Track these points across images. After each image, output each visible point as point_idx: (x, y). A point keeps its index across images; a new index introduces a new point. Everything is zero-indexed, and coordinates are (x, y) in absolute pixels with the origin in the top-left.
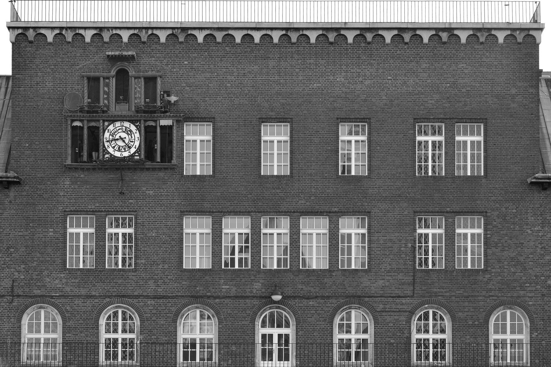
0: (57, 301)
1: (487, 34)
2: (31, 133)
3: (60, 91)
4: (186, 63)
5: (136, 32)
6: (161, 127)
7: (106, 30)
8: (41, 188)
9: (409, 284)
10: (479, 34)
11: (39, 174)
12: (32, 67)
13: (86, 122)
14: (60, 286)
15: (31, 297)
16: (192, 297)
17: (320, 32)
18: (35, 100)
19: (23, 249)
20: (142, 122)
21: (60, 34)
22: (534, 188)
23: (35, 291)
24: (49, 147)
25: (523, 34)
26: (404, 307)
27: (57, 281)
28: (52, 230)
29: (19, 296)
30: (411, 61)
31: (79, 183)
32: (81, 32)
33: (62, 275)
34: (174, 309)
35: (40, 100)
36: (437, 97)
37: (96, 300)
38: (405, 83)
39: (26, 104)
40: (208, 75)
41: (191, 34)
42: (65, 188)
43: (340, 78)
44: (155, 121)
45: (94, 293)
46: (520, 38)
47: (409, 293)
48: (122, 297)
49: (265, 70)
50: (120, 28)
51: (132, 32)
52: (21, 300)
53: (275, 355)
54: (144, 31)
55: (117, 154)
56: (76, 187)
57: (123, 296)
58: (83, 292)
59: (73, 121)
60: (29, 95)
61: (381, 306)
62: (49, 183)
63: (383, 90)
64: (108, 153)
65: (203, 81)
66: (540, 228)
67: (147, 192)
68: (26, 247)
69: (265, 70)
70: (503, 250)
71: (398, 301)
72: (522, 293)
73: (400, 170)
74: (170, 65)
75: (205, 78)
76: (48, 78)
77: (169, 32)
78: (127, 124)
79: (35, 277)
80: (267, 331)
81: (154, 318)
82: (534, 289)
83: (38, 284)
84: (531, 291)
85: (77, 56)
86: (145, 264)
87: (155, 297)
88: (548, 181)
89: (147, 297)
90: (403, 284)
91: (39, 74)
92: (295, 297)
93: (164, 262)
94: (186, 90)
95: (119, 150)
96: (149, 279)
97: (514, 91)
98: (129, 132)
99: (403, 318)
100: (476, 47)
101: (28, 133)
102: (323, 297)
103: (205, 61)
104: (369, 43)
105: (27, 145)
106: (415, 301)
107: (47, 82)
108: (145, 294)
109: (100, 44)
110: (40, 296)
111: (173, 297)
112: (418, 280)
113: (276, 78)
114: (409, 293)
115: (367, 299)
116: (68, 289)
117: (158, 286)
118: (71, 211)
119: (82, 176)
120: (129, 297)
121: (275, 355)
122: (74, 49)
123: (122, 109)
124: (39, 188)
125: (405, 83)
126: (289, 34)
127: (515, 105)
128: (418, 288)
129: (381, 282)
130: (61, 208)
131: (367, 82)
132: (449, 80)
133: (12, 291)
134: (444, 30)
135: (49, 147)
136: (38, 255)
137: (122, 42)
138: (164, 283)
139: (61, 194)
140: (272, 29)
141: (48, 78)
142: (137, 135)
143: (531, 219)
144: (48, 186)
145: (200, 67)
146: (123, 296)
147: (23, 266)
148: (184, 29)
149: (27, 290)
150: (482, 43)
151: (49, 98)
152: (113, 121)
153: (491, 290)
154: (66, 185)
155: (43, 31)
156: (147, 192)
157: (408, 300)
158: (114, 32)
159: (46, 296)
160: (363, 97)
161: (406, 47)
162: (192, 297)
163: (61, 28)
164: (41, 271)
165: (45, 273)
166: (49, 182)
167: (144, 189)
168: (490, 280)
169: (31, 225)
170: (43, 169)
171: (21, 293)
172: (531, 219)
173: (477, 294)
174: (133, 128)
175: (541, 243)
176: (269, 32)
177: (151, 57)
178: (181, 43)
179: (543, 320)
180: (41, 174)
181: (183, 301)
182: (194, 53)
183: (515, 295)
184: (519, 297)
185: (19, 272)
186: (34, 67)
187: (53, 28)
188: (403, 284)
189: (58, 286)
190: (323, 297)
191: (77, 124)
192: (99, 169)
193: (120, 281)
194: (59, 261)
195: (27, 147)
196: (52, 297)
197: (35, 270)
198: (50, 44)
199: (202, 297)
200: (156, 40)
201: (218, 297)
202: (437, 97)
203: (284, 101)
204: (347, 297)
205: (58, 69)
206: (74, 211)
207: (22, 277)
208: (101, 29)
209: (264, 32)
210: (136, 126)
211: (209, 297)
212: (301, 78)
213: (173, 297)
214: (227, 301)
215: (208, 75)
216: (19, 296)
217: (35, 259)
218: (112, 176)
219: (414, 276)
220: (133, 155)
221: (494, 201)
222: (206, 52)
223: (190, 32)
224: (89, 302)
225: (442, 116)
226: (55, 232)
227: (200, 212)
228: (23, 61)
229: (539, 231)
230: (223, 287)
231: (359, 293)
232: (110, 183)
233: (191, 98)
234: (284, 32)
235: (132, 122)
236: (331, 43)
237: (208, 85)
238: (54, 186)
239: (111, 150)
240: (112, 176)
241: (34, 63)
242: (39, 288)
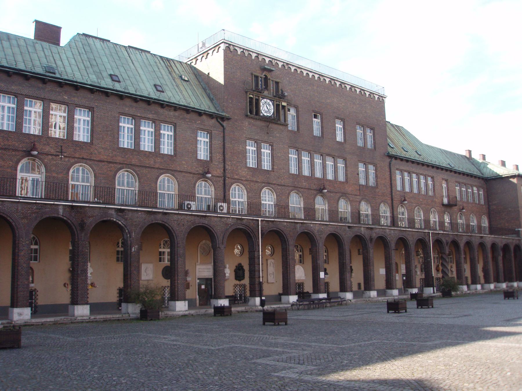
5: (271, 60)
7: (260, 55)
13: (254, 96)
14: (245, 175)
15: (233, 179)
16: (294, 187)
19: (229, 154)
20: (275, 102)
21: (243, 52)
23: (235, 176)
24: (239, 104)
26: (358, 200)
27: (244, 172)
28: (241, 146)
31: (251, 125)
33: (246, 170)
34: (288, 192)
37: (259, 184)
40: (295, 87)
41: (289, 67)
44: (279, 102)
45: (258, 181)
47: (358, 194)
54: (274, 60)
55: (265, 114)
56: (250, 126)
58: (254, 179)
59: (250, 94)
61: (351, 199)
64: (262, 113)
67: (277, 135)
68: (231, 153)
70: (381, 180)
71: (356, 197)
72: (387, 198)
78: (268, 101)
79: (235, 169)
81: (281, 195)
83: (236, 173)
89: (278, 185)
91: (235, 68)
95: (266, 112)
99: (357, 204)
108: (277, 183)
109: (257, 61)
110: (237, 179)
114: (358, 194)
115: (347, 195)
116: (248, 177)
118: (248, 138)
119: (252, 122)
120: (272, 184)
122: (247, 60)
126: (320, 77)
130: (244, 136)
135: (239, 104)
136: (236, 158)
137: (266, 62)
139: (245, 129)
142: (272, 107)
146: (269, 183)
147: (230, 163)
148: (287, 64)
149: (232, 175)
151: (239, 81)
152: (264, 98)
155: (236, 48)
156: (277, 135)
158: (264, 57)
159: (240, 179)
161: (352, 93)
162: (294, 187)
165: (239, 167)
167: (275, 133)
169: (233, 142)
171: (229, 177)
174: (271, 103)
176: (314, 74)
178: (286, 70)
181: (291, 188)
184: (386, 199)
185: (228, 165)
187: (240, 48)
189: (244, 175)
191: (252, 96)
192: (261, 120)
193: (268, 176)
196: (242, 180)
200: (277, 66)
201: (302, 188)
203: (320, 105)
204: (342, 193)
206: (250, 138)
207: (230, 168)
210: (272, 103)
217: (235, 160)
223: (289, 66)
230: (304, 184)
232: (263, 127)
234: (319, 76)
235: (271, 100)
238: (242, 124)
239: (263, 111)
240: (264, 124)
242: (237, 175)
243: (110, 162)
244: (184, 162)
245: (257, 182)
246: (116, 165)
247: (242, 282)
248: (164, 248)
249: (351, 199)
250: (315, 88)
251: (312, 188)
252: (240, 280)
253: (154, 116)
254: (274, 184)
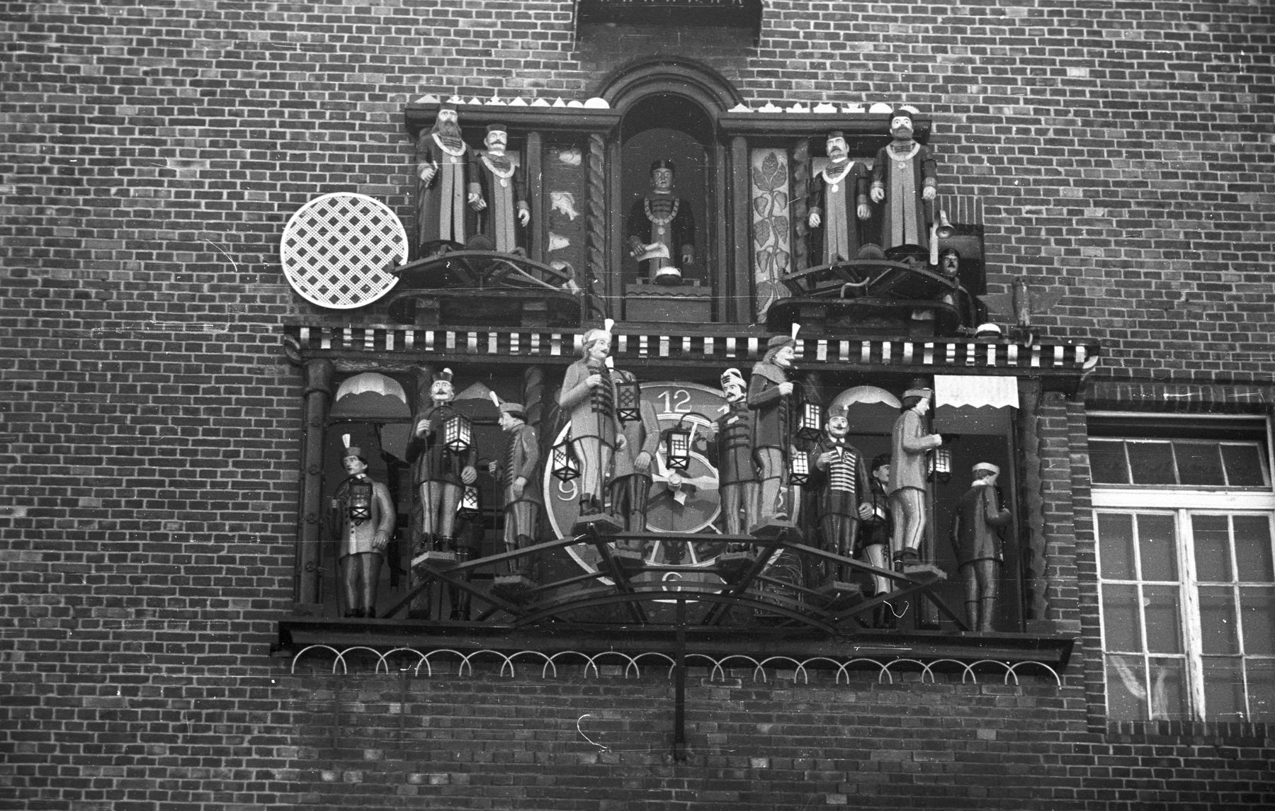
2: (47, 439)
3: (260, 207)
4: (1073, 73)
8: (99, 783)
11: (91, 691)
12: (77, 69)
18: (86, 255)
24: (171, 526)
35: (122, 255)
39: (24, 273)
42: (274, 787)
60: (52, 221)
62: (161, 750)
65: (1194, 176)
74: (973, 81)
75: (1205, 156)
76: (184, 133)
85: (377, 21)
91: (125, 110)
94: (1089, 222)
101: (28, 439)
103: (1199, 68)
105: (21, 512)
107: (171, 153)
124: (85, 783)
141: (184, 133)
144: (155, 773)
145: (1173, 96)
154: (280, 764)
166: (157, 746)
170: (125, 659)
177: (849, 37)
180: (106, 691)
182: (1130, 25)
186: (90, 69)
195: (19, 522)
205: (251, 85)
218: (608, 715)
222: (1205, 19)
228: (22, 37)
233: (1125, 264)
237: (1234, 198)
238: (191, 773)
241: (92, 51)
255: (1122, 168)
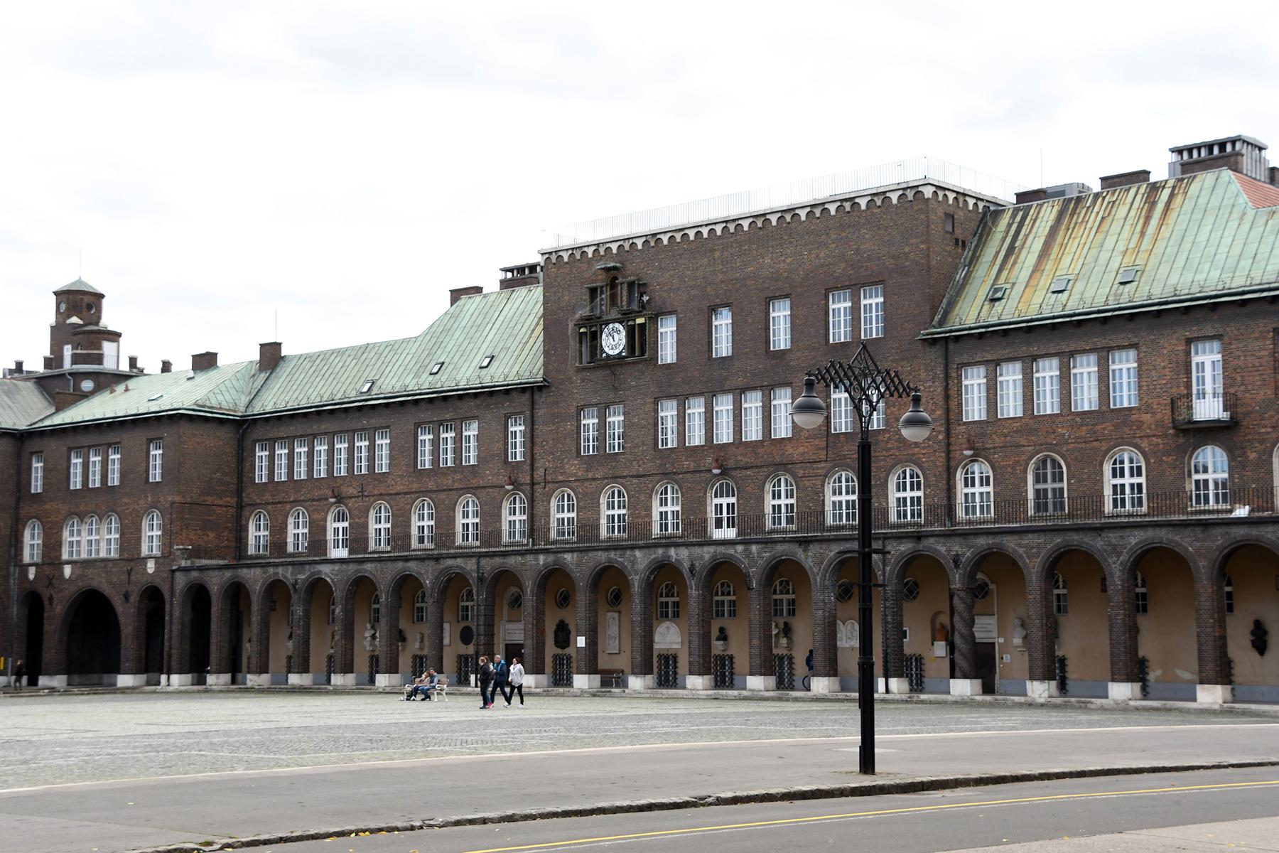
0: (573, 485)
1: (883, 197)
6: (639, 324)
9: (823, 449)
10: (875, 199)
17: (751, 220)
22: (926, 344)
25: (913, 192)
29: (549, 482)
30: (823, 234)
32: (585, 249)
34: (650, 486)
36: (843, 265)
38: (818, 256)
43: (768, 260)
46: (910, 197)
47: (824, 457)
48: (615, 478)
49: (711, 262)
50: (611, 242)
51: (619, 243)
52: (550, 485)
53: (725, 523)
55: (611, 353)
57: (616, 477)
58: (590, 475)
61: (802, 472)
63: (800, 266)
66: (931, 383)
68: (553, 440)
69: (711, 262)
71: (815, 466)
73: (815, 340)
77: (644, 239)
78: (617, 325)
80: (718, 501)
82: (926, 445)
84: (924, 448)
86: (630, 448)
87: (637, 476)
88: (930, 337)
89: (632, 476)
90: (819, 449)
92: (736, 469)
93: (643, 444)
96: (634, 460)
97: (907, 249)
98: (618, 332)
99: (819, 482)
100: (875, 211)
102: (757, 467)
104: (789, 223)
106: (828, 465)
111: (649, 475)
112: (830, 444)
113: (721, 267)
114: (824, 457)
115: (790, 466)
117: (640, 466)
120: (620, 477)
121: (725, 523)
123: (614, 314)
125: (818, 256)
127: (908, 263)
128: (830, 452)
129: (801, 449)
131: (788, 260)
132: (853, 247)
133: (545, 479)
134: (846, 200)
138: (644, 463)
140: (715, 223)
143: (923, 375)
146: (616, 477)
148: (654, 235)
150: (879, 207)
152: (608, 324)
153: (890, 449)
157: (823, 465)
160: (785, 274)
163: (573, 249)
164: (563, 459)
168: (889, 439)
172: (923, 375)
173: (878, 454)
174: (621, 328)
175: (932, 399)
176: (713, 227)
179: (935, 476)
181: (657, 478)
183: (911, 452)
184: (913, 454)
187: (567, 250)
188: (819, 449)
190: (757, 467)
191: (582, 330)
193: (614, 464)
194: (574, 449)
197: (559, 460)
198: (567, 263)
199: (669, 473)
202: (843, 265)
208: (598, 245)
209: (710, 227)
211: (675, 473)
212: (738, 264)
213: (649, 475)
214: (687, 475)
215: (672, 273)
216: (549, 482)
219: (827, 440)
220: (621, 352)
221: (891, 361)
224: (594, 484)
225: (847, 283)
226: (571, 425)
227: (669, 397)
229: (930, 387)
231: (784, 462)
234: (724, 225)
236: (760, 228)
243: (406, 493)
244: (487, 472)
245: (594, 479)
246: (412, 495)
247: (567, 651)
248: (467, 601)
249: (802, 472)
250: (717, 254)
251: (702, 468)
252: (563, 648)
253: (452, 414)
254: (625, 477)
255: (661, 279)
